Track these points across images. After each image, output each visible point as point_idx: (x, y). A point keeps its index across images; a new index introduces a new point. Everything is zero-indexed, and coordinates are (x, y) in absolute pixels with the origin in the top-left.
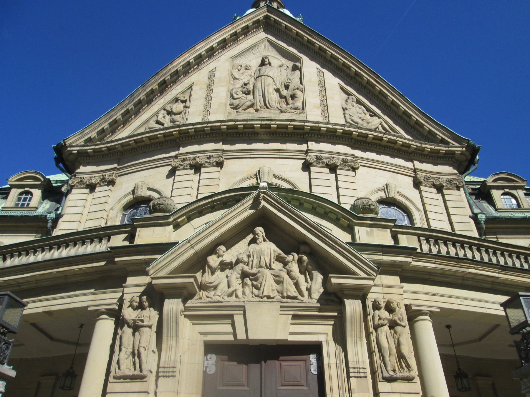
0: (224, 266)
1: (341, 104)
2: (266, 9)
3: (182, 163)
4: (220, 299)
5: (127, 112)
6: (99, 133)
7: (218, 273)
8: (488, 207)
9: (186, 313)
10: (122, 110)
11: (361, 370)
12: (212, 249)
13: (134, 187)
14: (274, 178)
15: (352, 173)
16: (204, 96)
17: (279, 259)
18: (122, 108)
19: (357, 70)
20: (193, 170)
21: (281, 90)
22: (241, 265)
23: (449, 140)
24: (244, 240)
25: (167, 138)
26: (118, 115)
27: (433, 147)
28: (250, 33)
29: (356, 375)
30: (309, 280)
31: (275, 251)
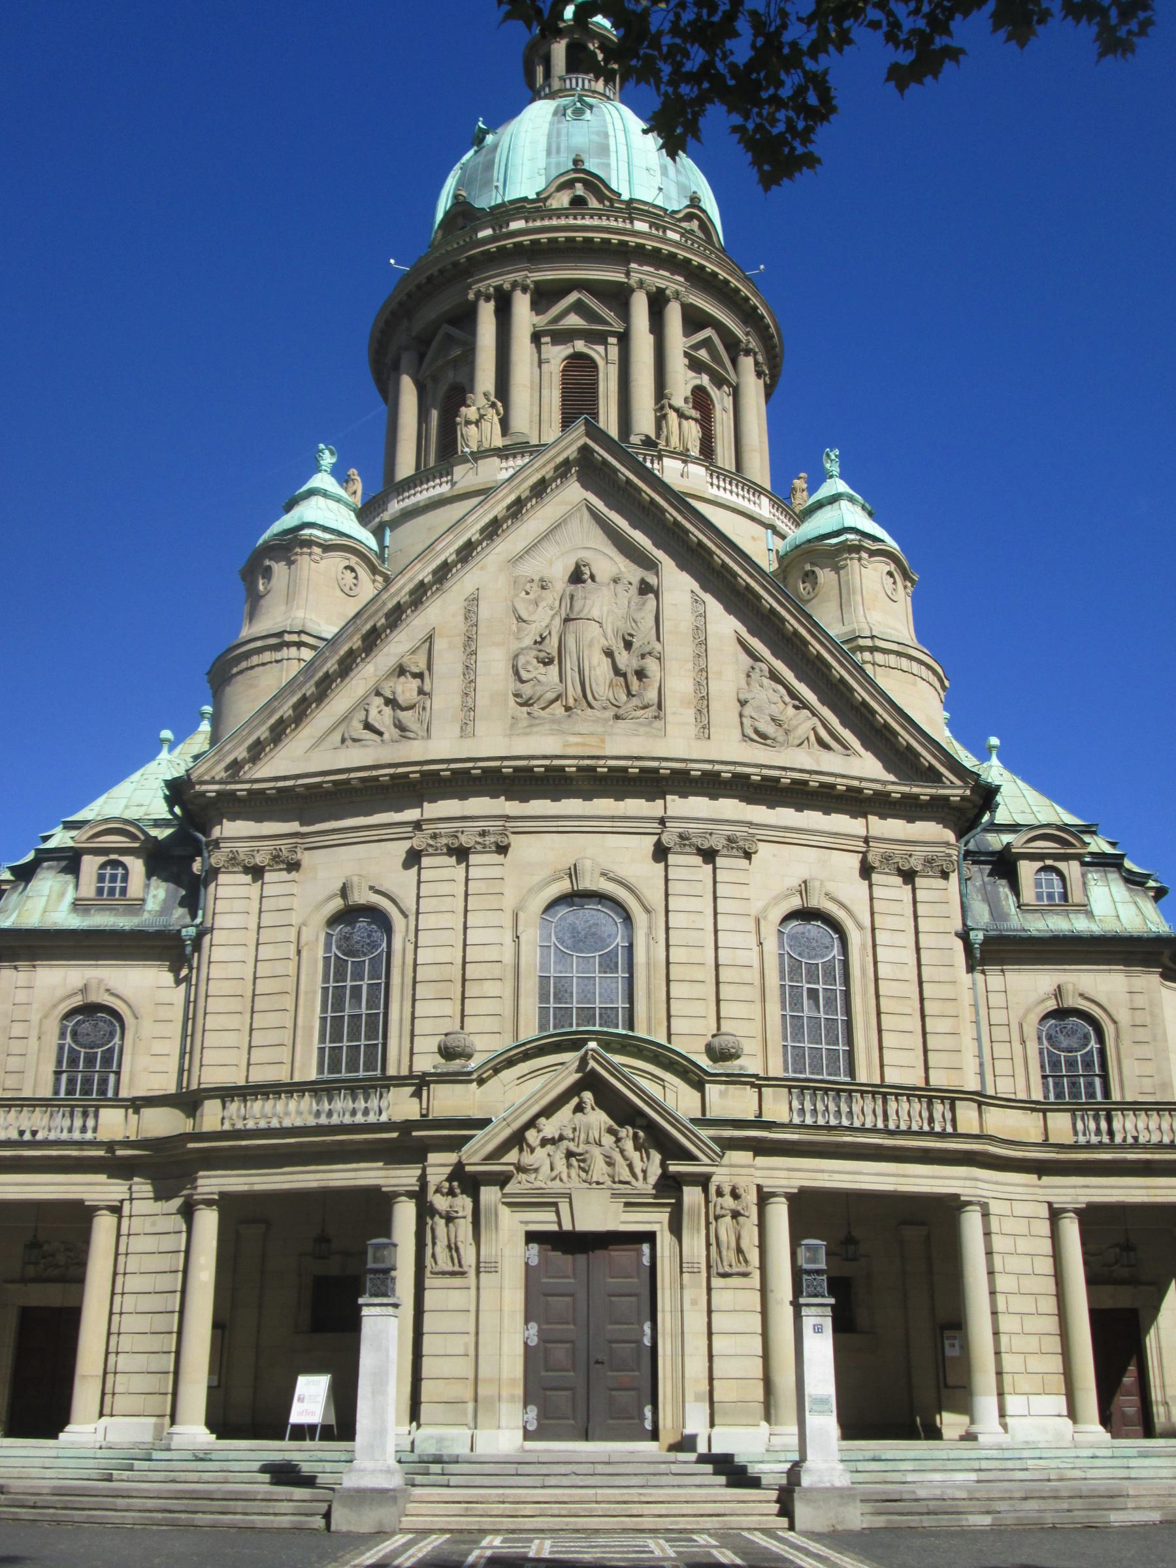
0: (544, 1142)
1: (735, 690)
2: (583, 428)
3: (431, 842)
4: (543, 1185)
5: (304, 699)
6: (250, 749)
7: (539, 1150)
8: (1007, 896)
9: (504, 1200)
10: (293, 695)
11: (696, 1265)
12: (531, 1123)
13: (344, 884)
14: (602, 879)
15: (744, 863)
16: (460, 668)
17: (610, 1131)
18: (293, 693)
19: (775, 605)
20: (454, 858)
21: (616, 654)
22: (565, 1143)
23: (942, 770)
24: (568, 1105)
25: (396, 781)
26: (285, 708)
27: (906, 789)
28: (549, 490)
29: (690, 1270)
30: (645, 1159)
31: (605, 1123)
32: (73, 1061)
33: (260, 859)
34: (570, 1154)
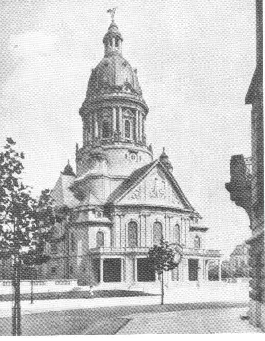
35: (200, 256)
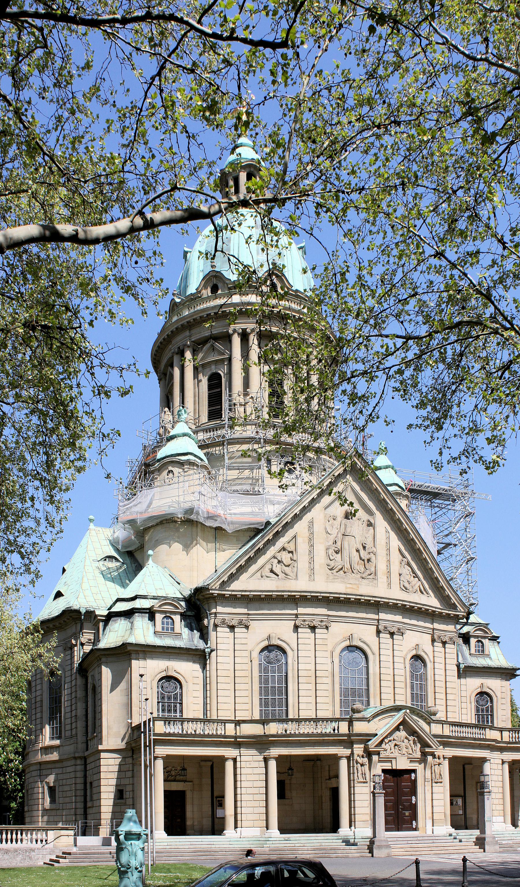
32: (163, 698)
33: (234, 623)
34: (396, 745)
35: (492, 748)
